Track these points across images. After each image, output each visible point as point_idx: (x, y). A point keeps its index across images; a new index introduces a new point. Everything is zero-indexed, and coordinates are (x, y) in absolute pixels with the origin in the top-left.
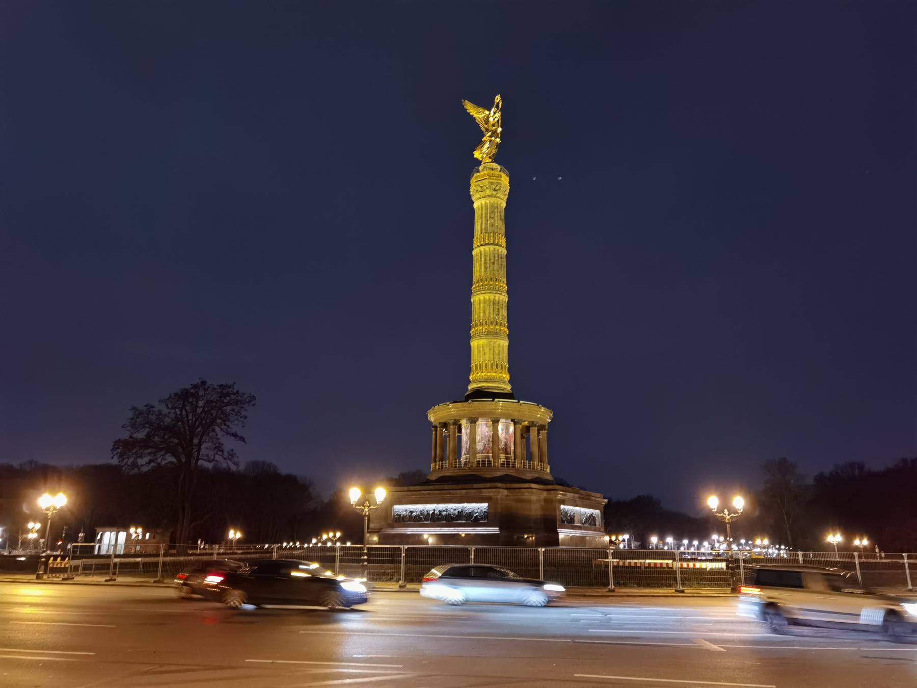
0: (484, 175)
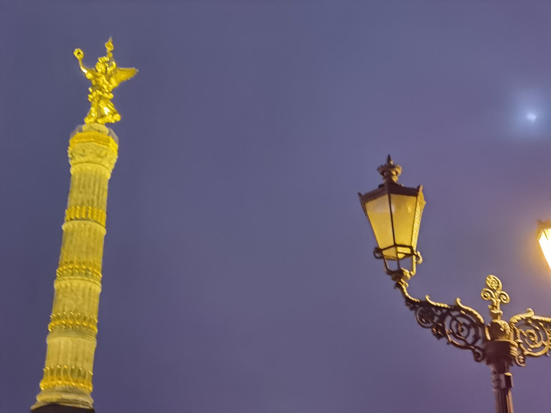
0: (89, 137)
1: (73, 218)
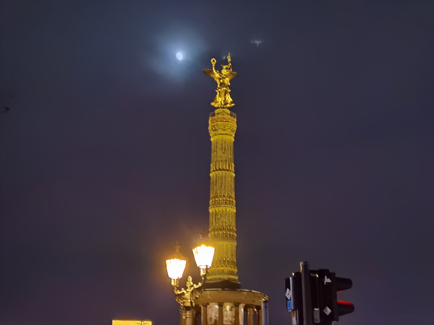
1: (215, 169)
